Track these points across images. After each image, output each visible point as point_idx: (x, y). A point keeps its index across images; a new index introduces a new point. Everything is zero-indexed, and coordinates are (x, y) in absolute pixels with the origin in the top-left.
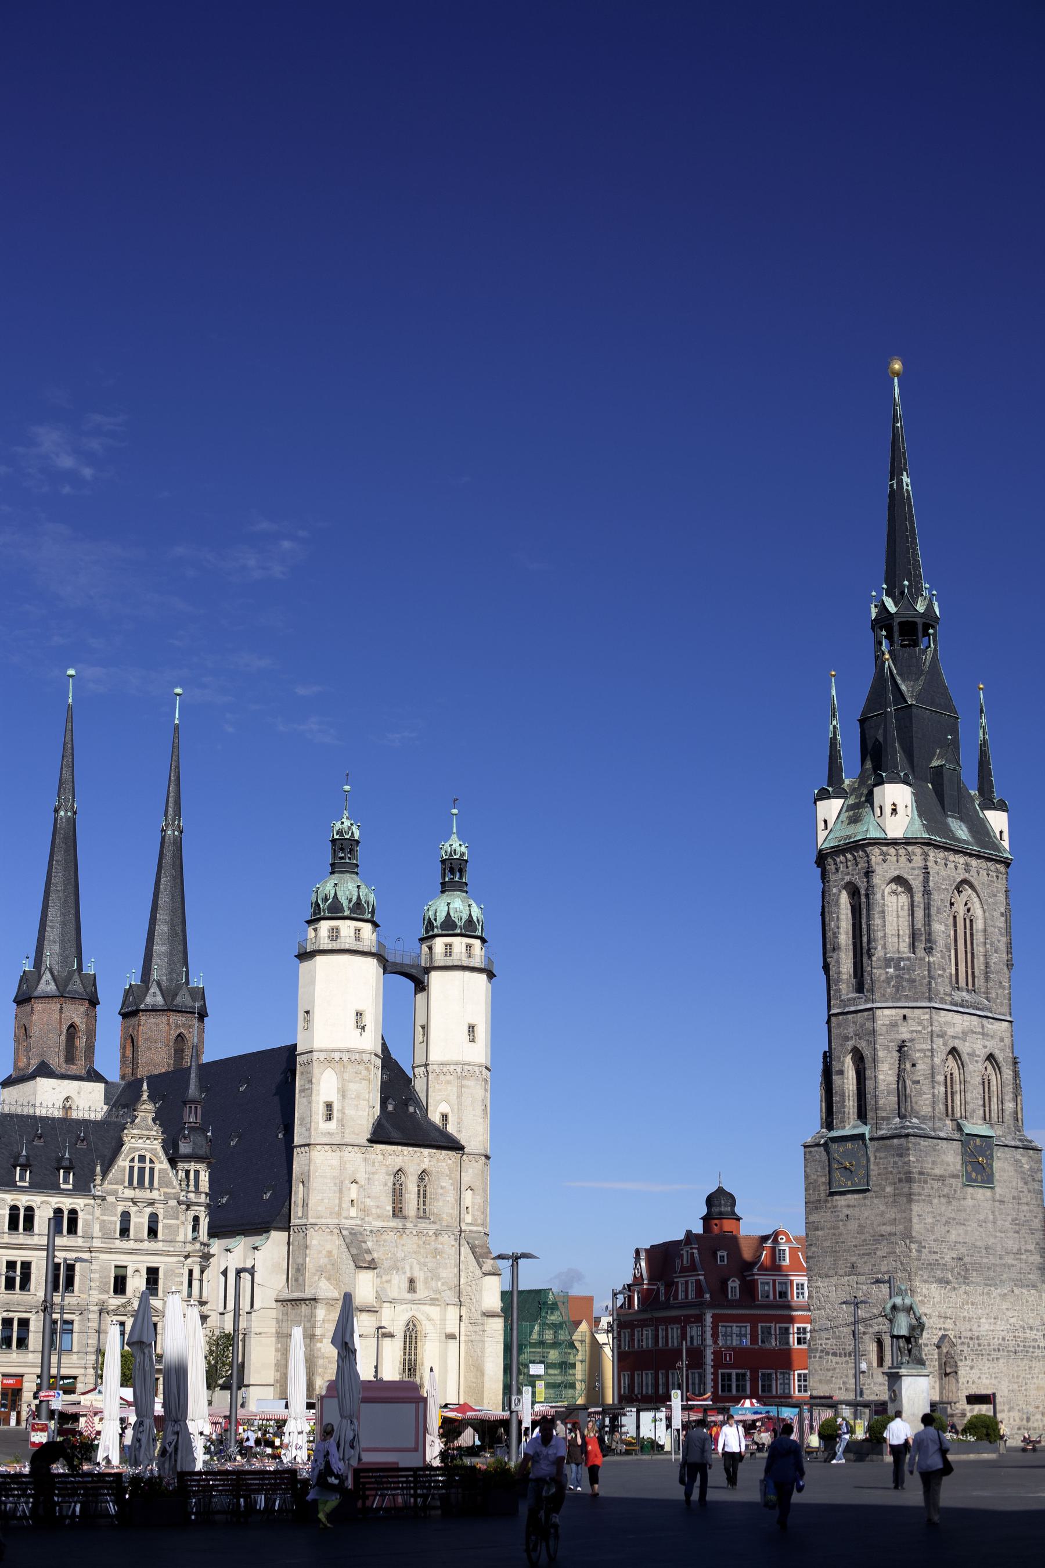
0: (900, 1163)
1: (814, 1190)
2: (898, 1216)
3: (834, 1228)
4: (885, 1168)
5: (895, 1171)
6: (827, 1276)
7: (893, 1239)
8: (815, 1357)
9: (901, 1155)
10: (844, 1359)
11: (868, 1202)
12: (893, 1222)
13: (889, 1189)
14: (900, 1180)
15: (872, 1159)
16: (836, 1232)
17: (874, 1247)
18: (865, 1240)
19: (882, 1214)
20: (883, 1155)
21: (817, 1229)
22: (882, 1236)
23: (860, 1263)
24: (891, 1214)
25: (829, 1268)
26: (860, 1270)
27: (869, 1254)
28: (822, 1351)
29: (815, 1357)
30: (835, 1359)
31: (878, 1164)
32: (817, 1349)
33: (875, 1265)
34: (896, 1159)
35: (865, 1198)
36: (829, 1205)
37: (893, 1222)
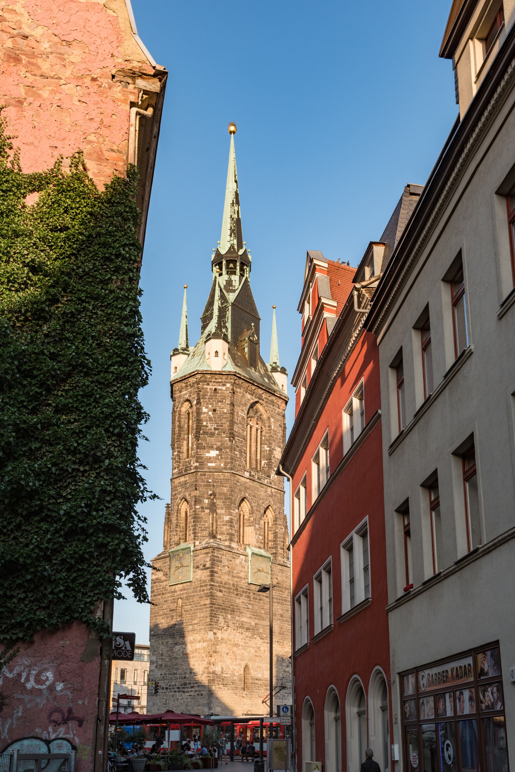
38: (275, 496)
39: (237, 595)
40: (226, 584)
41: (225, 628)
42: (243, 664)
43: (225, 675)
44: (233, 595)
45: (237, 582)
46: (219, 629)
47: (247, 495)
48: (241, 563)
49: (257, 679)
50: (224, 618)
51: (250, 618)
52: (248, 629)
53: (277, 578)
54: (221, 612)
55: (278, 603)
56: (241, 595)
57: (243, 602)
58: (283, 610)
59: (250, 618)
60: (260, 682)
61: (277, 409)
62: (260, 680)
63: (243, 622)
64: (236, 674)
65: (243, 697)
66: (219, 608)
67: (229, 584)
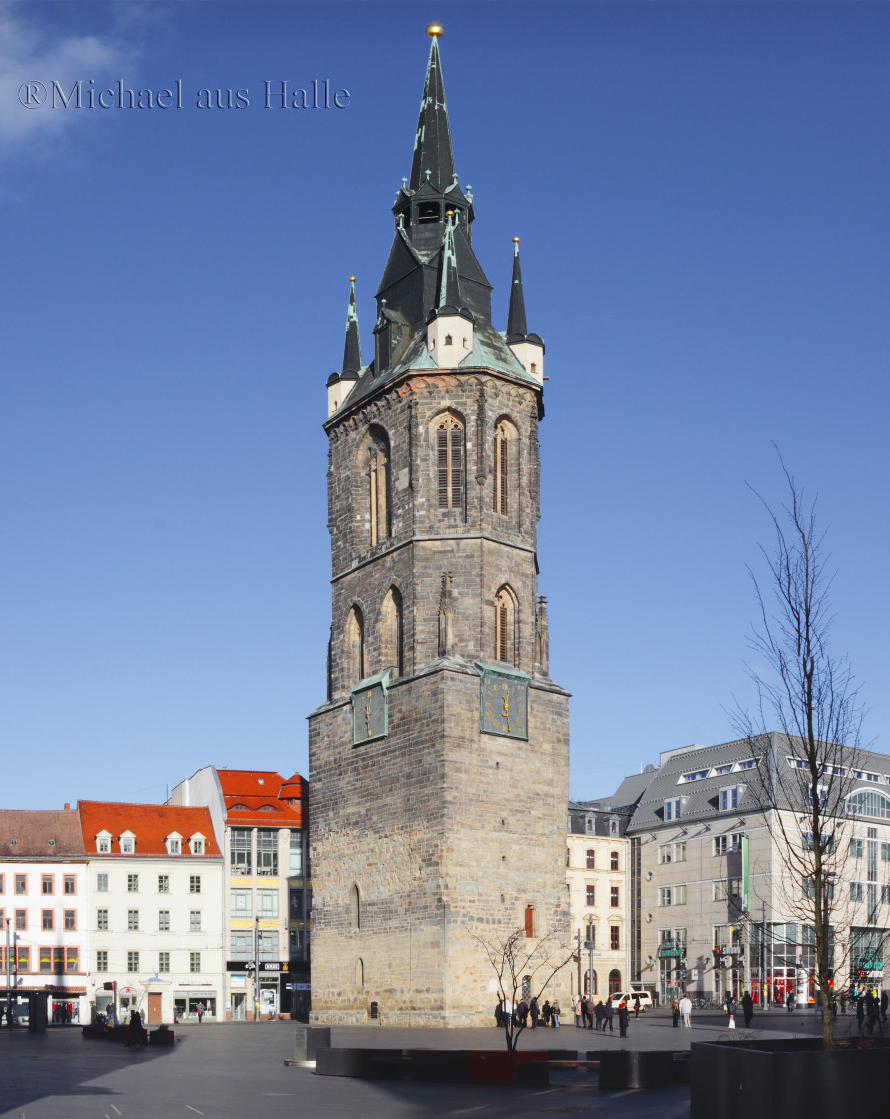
0: (559, 723)
1: (457, 724)
2: (556, 778)
3: (481, 773)
4: (543, 723)
5: (554, 729)
6: (471, 828)
7: (550, 801)
8: (455, 921)
9: (560, 714)
10: (492, 926)
11: (523, 755)
12: (550, 783)
13: (547, 747)
14: (559, 741)
15: (529, 708)
16: (485, 779)
17: (528, 805)
18: (517, 796)
19: (538, 772)
20: (540, 708)
21: (459, 770)
22: (538, 794)
23: (511, 820)
24: (548, 773)
25: (474, 820)
26: (511, 827)
27: (521, 812)
28: (464, 915)
29: (455, 921)
30: (481, 926)
31: (535, 716)
32: (458, 913)
33: (529, 825)
34: (556, 717)
35: (520, 748)
36: (475, 746)
37: (550, 783)
38: (399, 561)
39: (340, 774)
40: (325, 765)
41: (326, 835)
42: (350, 883)
43: (328, 908)
44: (336, 778)
45: (340, 753)
46: (318, 840)
47: (355, 598)
48: (344, 719)
49: (370, 905)
50: (325, 820)
51: (359, 803)
52: (357, 823)
53: (400, 711)
54: (322, 812)
55: (403, 755)
56: (346, 772)
57: (348, 783)
58: (411, 764)
59: (359, 803)
60: (374, 909)
61: (400, 405)
62: (373, 904)
63: (348, 815)
64: (341, 903)
65: (351, 937)
66: (318, 808)
67: (330, 763)
